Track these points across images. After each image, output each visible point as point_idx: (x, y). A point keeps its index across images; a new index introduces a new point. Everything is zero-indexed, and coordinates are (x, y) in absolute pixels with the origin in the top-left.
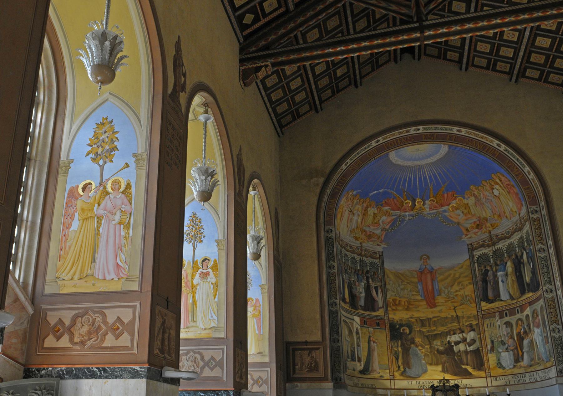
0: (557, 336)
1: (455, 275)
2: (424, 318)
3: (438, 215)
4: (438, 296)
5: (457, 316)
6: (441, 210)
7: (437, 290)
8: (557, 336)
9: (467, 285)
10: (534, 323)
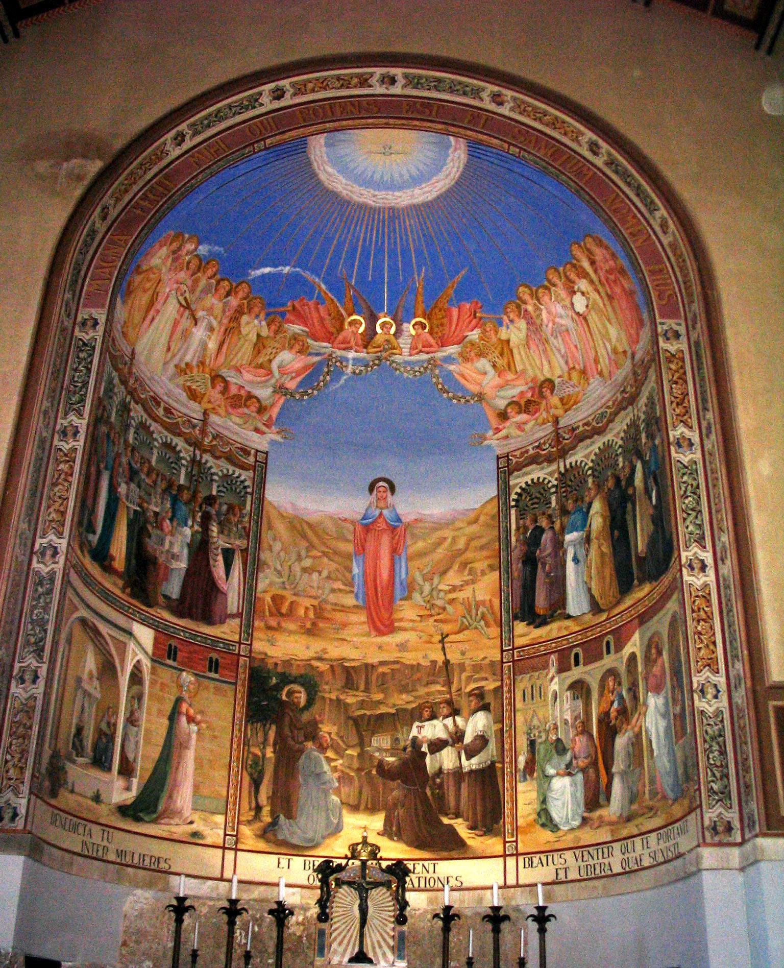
0: (711, 709)
4: (401, 600)
5: (447, 663)
6: (439, 355)
7: (401, 584)
8: (710, 710)
9: (483, 573)
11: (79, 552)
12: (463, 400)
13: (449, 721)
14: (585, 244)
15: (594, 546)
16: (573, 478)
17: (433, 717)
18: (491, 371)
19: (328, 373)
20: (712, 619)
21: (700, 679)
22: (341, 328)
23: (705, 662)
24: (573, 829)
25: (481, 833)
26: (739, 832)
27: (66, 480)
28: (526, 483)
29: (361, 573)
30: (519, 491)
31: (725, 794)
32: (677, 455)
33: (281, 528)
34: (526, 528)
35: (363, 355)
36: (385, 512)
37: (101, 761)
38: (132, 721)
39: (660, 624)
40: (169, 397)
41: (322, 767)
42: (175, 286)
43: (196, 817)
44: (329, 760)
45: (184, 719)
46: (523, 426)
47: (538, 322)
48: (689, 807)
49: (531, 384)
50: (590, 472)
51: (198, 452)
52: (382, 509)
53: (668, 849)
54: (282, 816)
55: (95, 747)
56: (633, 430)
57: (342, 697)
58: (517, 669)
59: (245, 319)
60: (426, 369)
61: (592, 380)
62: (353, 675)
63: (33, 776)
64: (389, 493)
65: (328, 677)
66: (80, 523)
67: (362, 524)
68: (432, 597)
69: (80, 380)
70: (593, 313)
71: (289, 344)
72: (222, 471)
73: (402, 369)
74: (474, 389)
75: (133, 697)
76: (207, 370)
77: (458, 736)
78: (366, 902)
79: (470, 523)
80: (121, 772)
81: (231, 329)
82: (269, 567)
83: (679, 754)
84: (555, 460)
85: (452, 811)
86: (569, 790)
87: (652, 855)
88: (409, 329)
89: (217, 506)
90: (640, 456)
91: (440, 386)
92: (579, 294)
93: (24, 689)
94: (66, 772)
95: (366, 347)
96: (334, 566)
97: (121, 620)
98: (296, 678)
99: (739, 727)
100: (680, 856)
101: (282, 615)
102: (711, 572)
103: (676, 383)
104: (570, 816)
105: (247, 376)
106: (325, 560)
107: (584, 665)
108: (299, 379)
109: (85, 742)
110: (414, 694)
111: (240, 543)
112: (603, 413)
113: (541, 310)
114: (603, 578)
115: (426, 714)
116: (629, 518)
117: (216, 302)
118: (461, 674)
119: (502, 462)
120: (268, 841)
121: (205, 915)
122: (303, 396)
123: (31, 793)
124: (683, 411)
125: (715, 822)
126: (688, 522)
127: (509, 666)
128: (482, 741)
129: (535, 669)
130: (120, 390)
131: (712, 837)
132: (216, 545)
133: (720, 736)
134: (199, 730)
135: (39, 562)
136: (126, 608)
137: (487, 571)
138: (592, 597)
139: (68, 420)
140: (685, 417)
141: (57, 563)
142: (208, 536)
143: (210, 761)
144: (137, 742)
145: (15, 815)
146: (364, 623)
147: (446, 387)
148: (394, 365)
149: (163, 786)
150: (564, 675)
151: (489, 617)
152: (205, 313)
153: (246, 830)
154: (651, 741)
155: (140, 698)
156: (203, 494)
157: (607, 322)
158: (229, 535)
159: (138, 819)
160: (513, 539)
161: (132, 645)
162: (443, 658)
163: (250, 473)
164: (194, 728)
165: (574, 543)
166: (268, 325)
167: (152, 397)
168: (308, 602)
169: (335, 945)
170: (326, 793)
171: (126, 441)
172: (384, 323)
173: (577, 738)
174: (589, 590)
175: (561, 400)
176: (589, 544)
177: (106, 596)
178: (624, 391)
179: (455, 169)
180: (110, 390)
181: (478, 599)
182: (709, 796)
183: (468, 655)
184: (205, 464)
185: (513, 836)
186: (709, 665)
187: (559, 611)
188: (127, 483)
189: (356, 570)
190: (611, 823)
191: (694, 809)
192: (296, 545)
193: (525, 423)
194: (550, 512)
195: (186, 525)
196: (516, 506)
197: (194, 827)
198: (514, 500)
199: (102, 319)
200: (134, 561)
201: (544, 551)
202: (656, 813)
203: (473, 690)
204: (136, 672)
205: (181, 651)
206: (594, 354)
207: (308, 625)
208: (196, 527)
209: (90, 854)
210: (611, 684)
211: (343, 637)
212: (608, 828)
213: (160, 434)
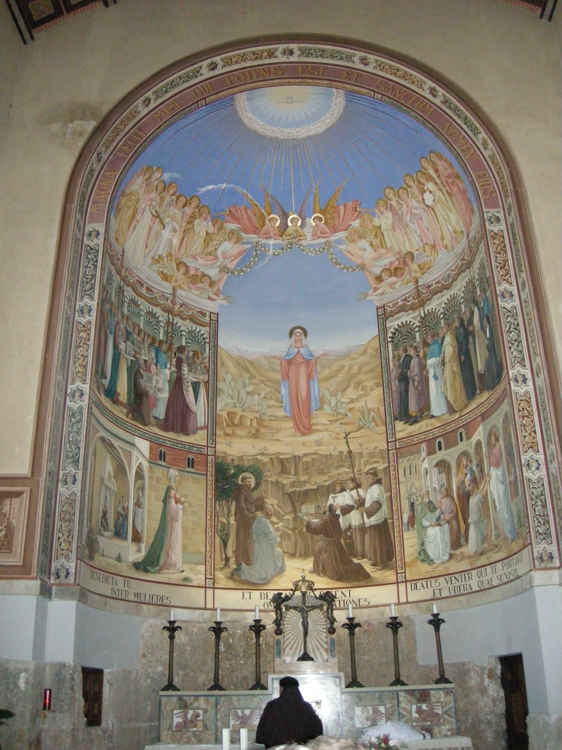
1: (350, 367)
2: (288, 456)
3: (328, 249)
4: (317, 410)
5: (350, 452)
6: (332, 238)
7: (315, 399)
8: (534, 478)
9: (372, 389)
10: (489, 458)
11: (97, 393)
12: (351, 270)
13: (354, 492)
14: (430, 158)
15: (448, 368)
16: (430, 321)
17: (343, 490)
18: (369, 249)
19: (256, 256)
20: (533, 415)
21: (526, 457)
22: (264, 224)
23: (529, 445)
24: (443, 563)
25: (381, 568)
26: (558, 559)
27: (85, 344)
28: (398, 325)
29: (287, 393)
30: (393, 331)
31: (547, 534)
32: (503, 303)
33: (230, 365)
34: (399, 356)
35: (280, 241)
36: (301, 350)
37: (120, 533)
38: (138, 504)
39: (497, 419)
40: (148, 279)
41: (269, 528)
42: (149, 203)
43: (185, 567)
44: (273, 523)
45: (173, 501)
46: (393, 285)
47: (400, 213)
48: (524, 544)
49: (397, 256)
50: (442, 316)
51: (171, 316)
52: (299, 348)
53: (510, 573)
54: (243, 563)
55: (116, 525)
56: (470, 287)
57: (279, 480)
58: (399, 455)
59: (197, 222)
60: (324, 249)
61: (440, 252)
62: (287, 464)
63: (78, 547)
64: (303, 336)
65: (269, 466)
66: (97, 372)
67: (286, 360)
68: (337, 407)
69: (90, 274)
70: (438, 204)
71: (229, 237)
72: (188, 328)
73: (307, 250)
74: (358, 261)
75: (138, 488)
76: (174, 259)
77: (361, 503)
78: (307, 620)
79: (360, 355)
80: (133, 540)
81: (188, 231)
82: (224, 393)
83: (514, 509)
84: (416, 309)
85: (360, 554)
86: (439, 535)
87: (499, 577)
88: (311, 222)
89: (186, 353)
90: (476, 303)
91: (334, 260)
92: (428, 193)
93: (67, 488)
94: (98, 542)
95: (281, 236)
96: (269, 389)
97: (127, 436)
98: (247, 468)
99: (555, 488)
100: (518, 577)
101: (235, 425)
102: (530, 382)
103: (499, 253)
104: (441, 554)
105: (201, 261)
106: (262, 385)
107: (445, 449)
108: (237, 261)
109: (109, 521)
110: (328, 475)
111: (204, 377)
112: (449, 275)
113: (402, 204)
114: (456, 389)
115: (338, 488)
116: (471, 347)
117: (177, 212)
118: (360, 460)
119: (381, 312)
120: (235, 581)
121: (196, 634)
122: (240, 272)
123: (77, 558)
124: (505, 272)
125: (541, 554)
126: (512, 350)
127: (393, 453)
128: (378, 505)
129: (411, 453)
130: (117, 279)
131: (540, 564)
132: (188, 380)
133: (542, 495)
134: (184, 508)
135: (71, 401)
136: (130, 428)
137: (374, 388)
138: (448, 402)
139: (84, 302)
140: (507, 277)
141: (83, 401)
142: (181, 373)
143: (192, 529)
144: (143, 519)
145: (68, 574)
146: (290, 428)
147: (338, 261)
148: (302, 247)
149: (162, 549)
150: (432, 457)
151: (378, 420)
152: (170, 220)
153: (220, 575)
154: (494, 501)
155: (143, 488)
156: (176, 346)
157: (449, 212)
158: (195, 373)
159: (147, 571)
160: (391, 365)
161: (135, 453)
162: (347, 449)
163: (207, 329)
164: (180, 507)
165: (433, 365)
166: (214, 225)
167: (137, 280)
168: (252, 416)
169: (287, 650)
170: (272, 546)
171: (122, 313)
172: (293, 219)
173: (443, 500)
174: (446, 398)
175: (419, 266)
176: (444, 365)
177: (115, 420)
178: (463, 259)
179: (337, 110)
180: (110, 279)
181: (369, 407)
182: (537, 536)
183: (364, 446)
184: (176, 324)
185: (402, 569)
186: (532, 447)
187: (426, 413)
188: (125, 342)
189: (283, 391)
190: (470, 557)
191: (527, 546)
192: (241, 376)
193: (395, 283)
194: (416, 344)
195: (166, 368)
196: (392, 341)
197: (185, 574)
198: (390, 337)
199: (102, 230)
200: (133, 396)
201: (414, 372)
202: (500, 549)
203: (369, 470)
204: (139, 470)
205: (168, 454)
206: (440, 234)
207: (253, 431)
208: (173, 369)
209: (117, 597)
210: (464, 462)
211: (277, 438)
212: (467, 561)
213: (144, 306)
